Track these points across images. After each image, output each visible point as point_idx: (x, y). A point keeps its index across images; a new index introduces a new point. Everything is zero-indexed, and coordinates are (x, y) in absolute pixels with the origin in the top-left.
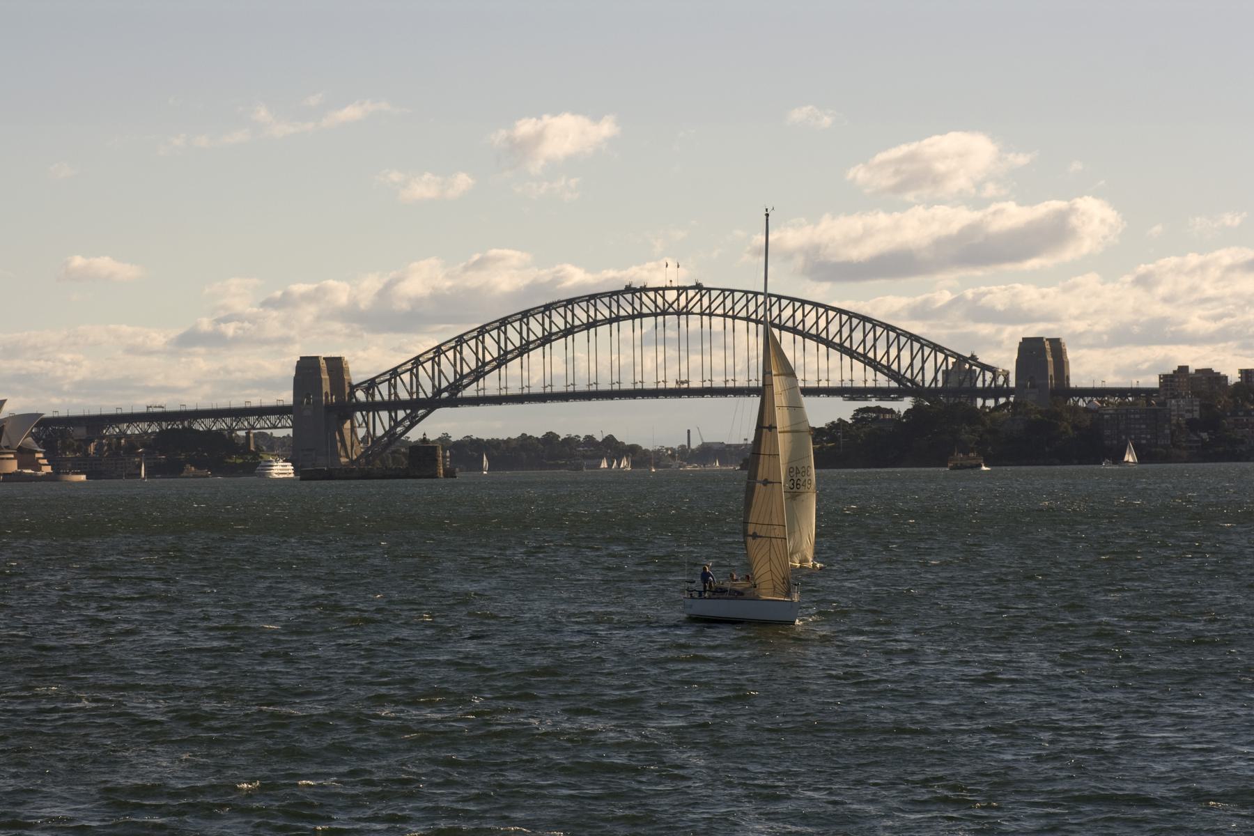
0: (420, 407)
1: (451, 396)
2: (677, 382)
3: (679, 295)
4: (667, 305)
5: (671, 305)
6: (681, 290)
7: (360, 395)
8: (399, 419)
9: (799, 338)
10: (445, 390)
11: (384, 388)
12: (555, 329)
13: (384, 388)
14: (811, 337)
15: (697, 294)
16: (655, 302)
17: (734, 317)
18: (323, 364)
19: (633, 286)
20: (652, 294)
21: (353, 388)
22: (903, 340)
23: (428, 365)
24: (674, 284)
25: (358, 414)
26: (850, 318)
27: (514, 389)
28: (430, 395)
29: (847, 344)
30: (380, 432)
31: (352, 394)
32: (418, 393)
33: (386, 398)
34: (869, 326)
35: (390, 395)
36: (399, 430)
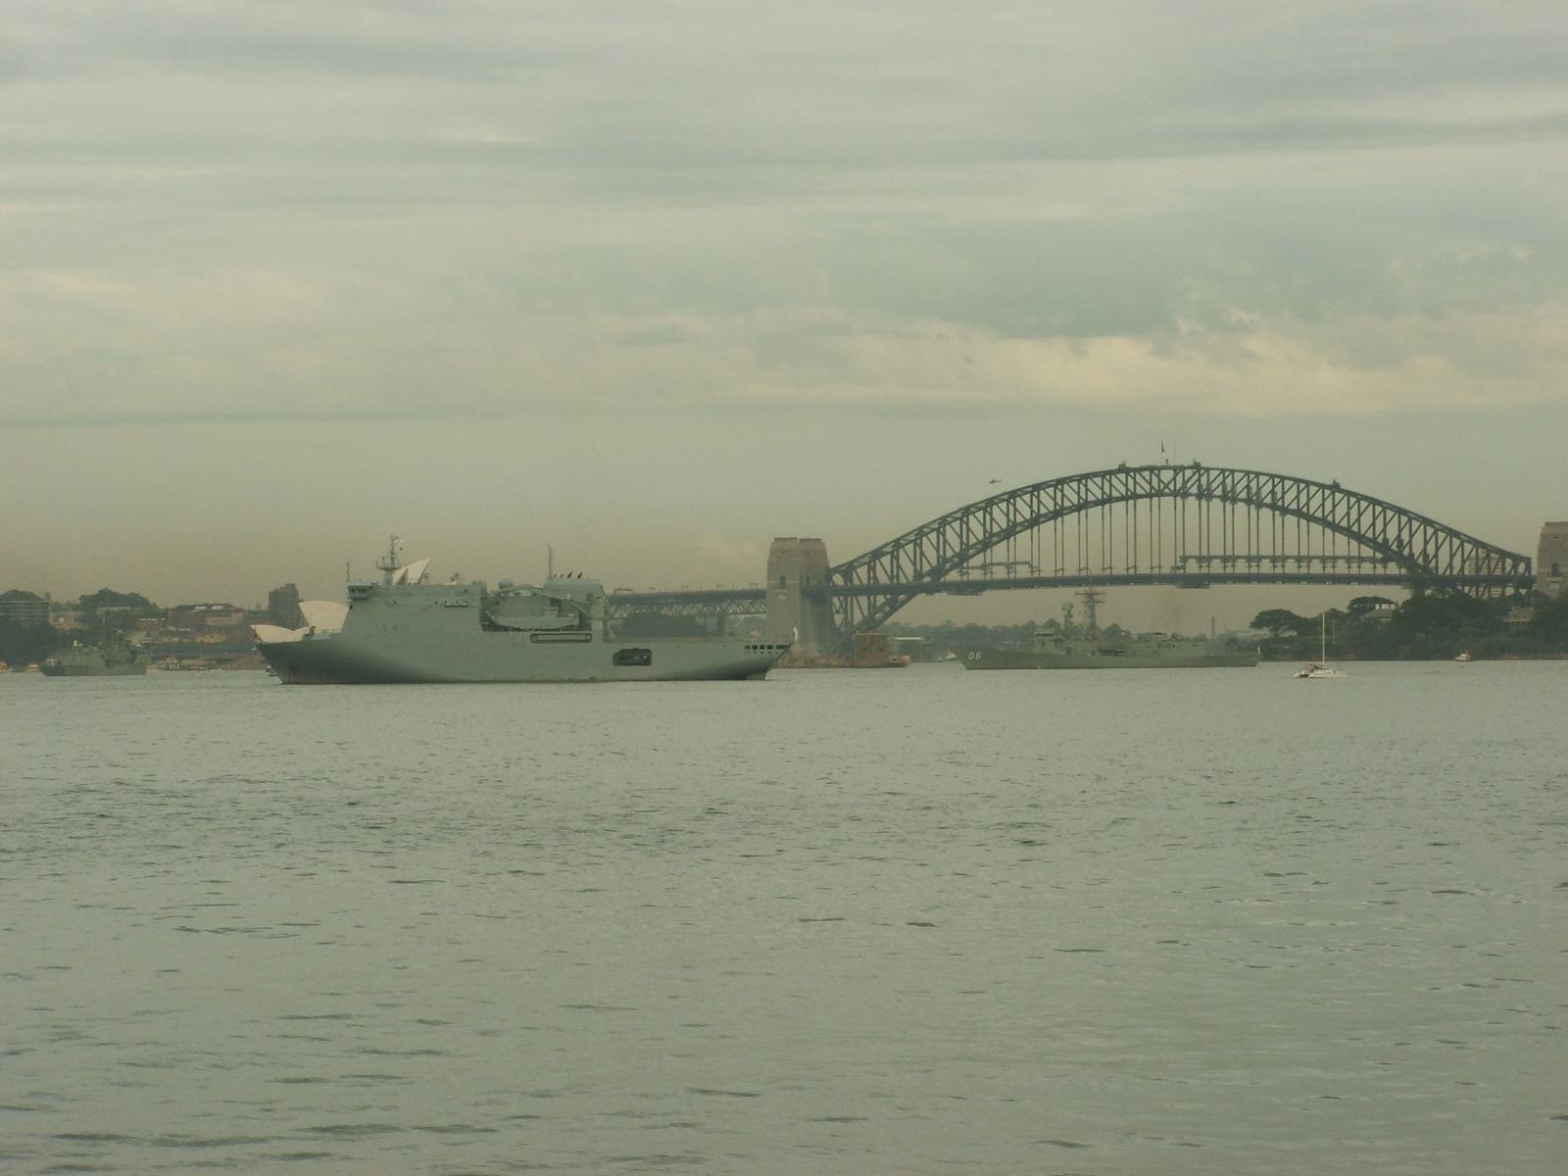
0: (899, 593)
1: (933, 583)
2: (1172, 568)
3: (1176, 474)
4: (1162, 485)
5: (1166, 486)
6: (1178, 469)
7: (838, 579)
8: (878, 604)
9: (1303, 522)
10: (928, 574)
11: (863, 571)
12: (1043, 511)
13: (863, 571)
14: (1316, 520)
15: (1194, 474)
16: (1150, 483)
19: (1127, 465)
20: (1146, 474)
21: (831, 572)
23: (910, 548)
24: (1172, 463)
26: (1358, 501)
27: (1000, 573)
30: (858, 618)
32: (898, 577)
33: (865, 582)
34: (1378, 509)
35: (869, 578)
36: (878, 616)
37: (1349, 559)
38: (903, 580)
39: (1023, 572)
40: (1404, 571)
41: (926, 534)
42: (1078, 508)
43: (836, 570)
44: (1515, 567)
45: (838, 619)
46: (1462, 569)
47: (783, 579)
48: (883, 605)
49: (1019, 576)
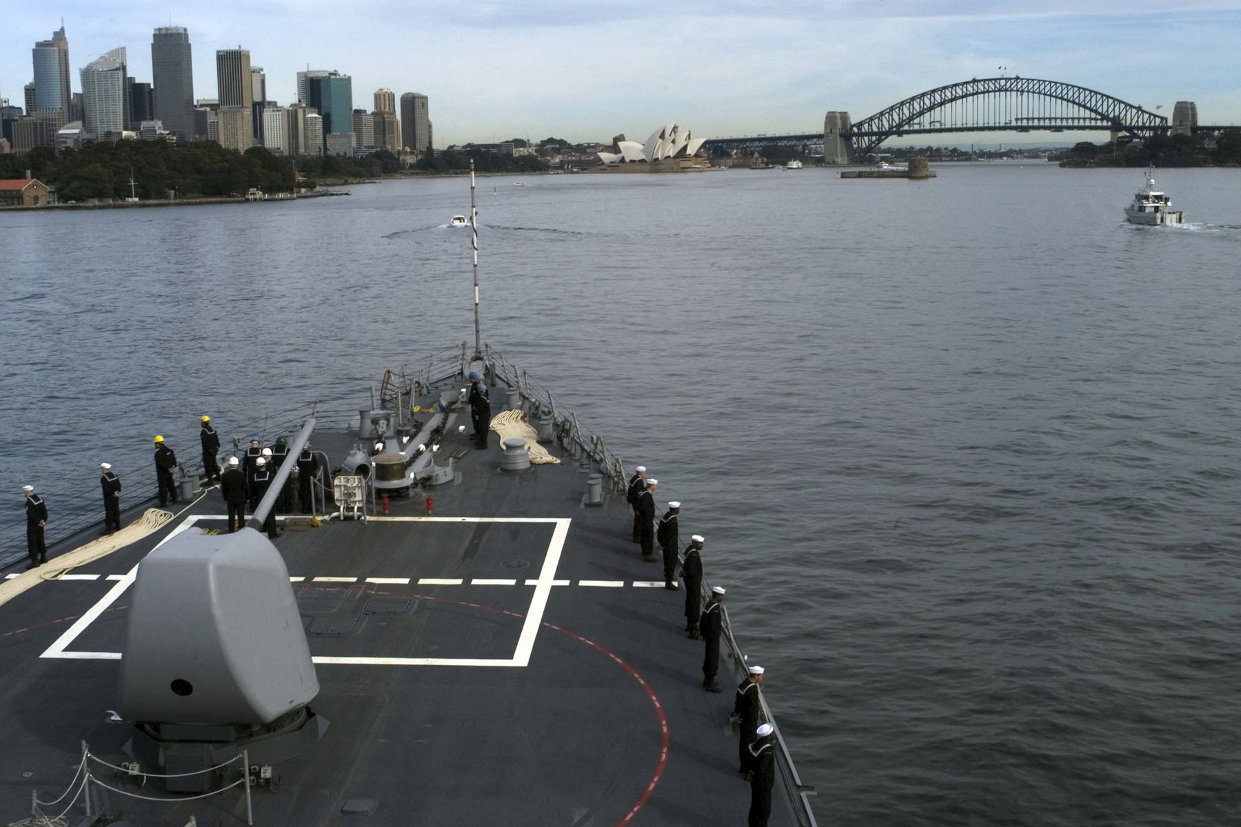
0: (882, 135)
7: (855, 129)
10: (895, 127)
11: (866, 126)
13: (866, 126)
17: (1034, 92)
18: (838, 115)
21: (852, 126)
22: (1116, 102)
25: (854, 138)
27: (927, 126)
28: (887, 129)
29: (1088, 105)
30: (864, 145)
31: (851, 129)
36: (873, 145)
37: (1084, 119)
38: (884, 129)
39: (937, 126)
40: (1110, 124)
41: (894, 109)
42: (962, 97)
43: (855, 125)
44: (1161, 122)
45: (855, 146)
46: (1137, 121)
47: (831, 130)
48: (875, 141)
49: (936, 127)
